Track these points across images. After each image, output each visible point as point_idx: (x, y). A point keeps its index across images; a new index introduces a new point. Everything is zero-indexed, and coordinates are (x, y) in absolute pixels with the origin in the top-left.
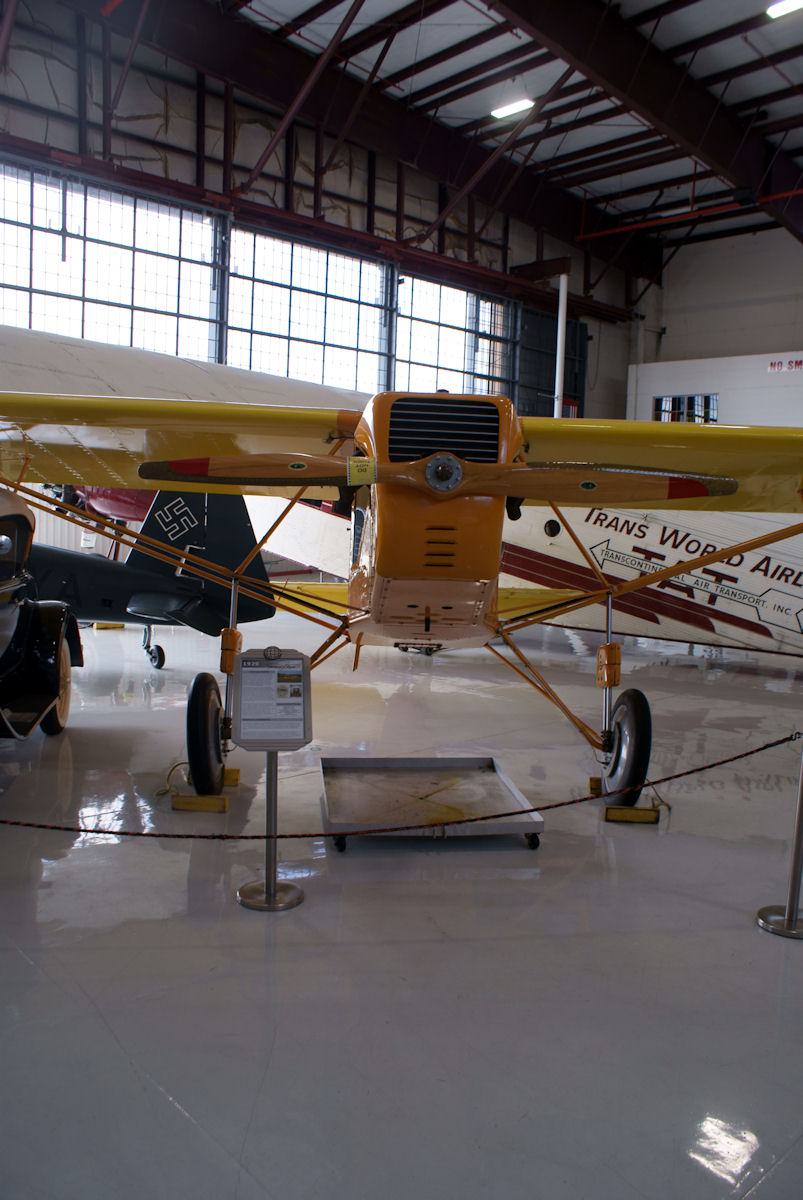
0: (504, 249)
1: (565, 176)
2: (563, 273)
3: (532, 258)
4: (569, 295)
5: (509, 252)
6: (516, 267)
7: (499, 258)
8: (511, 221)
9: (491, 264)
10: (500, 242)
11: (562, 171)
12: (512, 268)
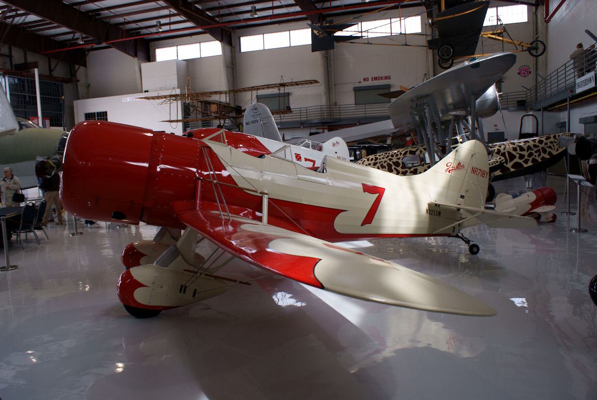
0: (10, 56)
1: (33, 29)
2: (36, 67)
3: (22, 61)
4: (40, 76)
5: (13, 58)
6: (17, 65)
7: (8, 60)
8: (12, 47)
9: (4, 64)
10: (8, 54)
11: (30, 27)
12: (15, 65)
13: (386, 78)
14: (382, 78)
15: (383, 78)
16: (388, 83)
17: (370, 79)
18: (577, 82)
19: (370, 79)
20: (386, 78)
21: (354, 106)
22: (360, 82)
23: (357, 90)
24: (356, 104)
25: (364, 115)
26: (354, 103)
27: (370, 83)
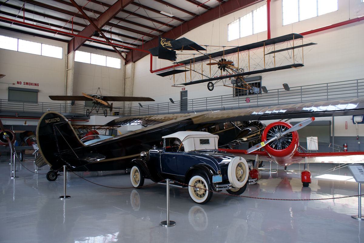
13: (36, 85)
14: (32, 84)
15: (33, 84)
16: (37, 89)
17: (23, 83)
18: (126, 106)
19: (23, 83)
20: (36, 85)
21: (7, 101)
22: (14, 84)
23: (10, 89)
24: (9, 100)
25: (22, 110)
26: (7, 99)
27: (22, 86)
